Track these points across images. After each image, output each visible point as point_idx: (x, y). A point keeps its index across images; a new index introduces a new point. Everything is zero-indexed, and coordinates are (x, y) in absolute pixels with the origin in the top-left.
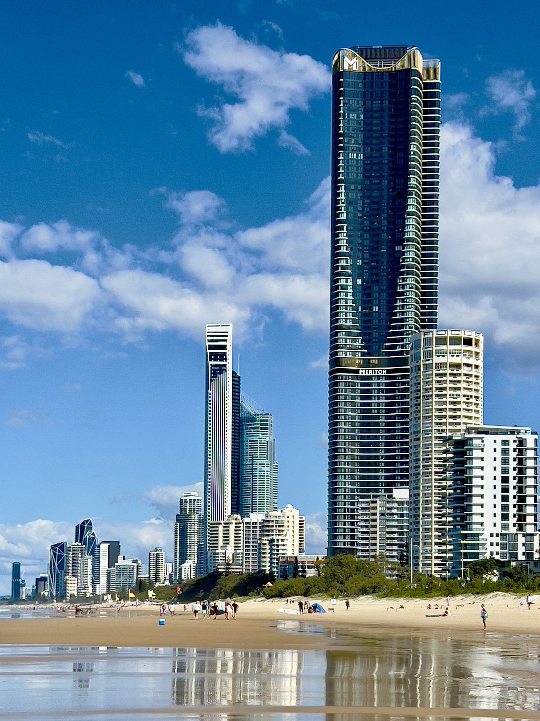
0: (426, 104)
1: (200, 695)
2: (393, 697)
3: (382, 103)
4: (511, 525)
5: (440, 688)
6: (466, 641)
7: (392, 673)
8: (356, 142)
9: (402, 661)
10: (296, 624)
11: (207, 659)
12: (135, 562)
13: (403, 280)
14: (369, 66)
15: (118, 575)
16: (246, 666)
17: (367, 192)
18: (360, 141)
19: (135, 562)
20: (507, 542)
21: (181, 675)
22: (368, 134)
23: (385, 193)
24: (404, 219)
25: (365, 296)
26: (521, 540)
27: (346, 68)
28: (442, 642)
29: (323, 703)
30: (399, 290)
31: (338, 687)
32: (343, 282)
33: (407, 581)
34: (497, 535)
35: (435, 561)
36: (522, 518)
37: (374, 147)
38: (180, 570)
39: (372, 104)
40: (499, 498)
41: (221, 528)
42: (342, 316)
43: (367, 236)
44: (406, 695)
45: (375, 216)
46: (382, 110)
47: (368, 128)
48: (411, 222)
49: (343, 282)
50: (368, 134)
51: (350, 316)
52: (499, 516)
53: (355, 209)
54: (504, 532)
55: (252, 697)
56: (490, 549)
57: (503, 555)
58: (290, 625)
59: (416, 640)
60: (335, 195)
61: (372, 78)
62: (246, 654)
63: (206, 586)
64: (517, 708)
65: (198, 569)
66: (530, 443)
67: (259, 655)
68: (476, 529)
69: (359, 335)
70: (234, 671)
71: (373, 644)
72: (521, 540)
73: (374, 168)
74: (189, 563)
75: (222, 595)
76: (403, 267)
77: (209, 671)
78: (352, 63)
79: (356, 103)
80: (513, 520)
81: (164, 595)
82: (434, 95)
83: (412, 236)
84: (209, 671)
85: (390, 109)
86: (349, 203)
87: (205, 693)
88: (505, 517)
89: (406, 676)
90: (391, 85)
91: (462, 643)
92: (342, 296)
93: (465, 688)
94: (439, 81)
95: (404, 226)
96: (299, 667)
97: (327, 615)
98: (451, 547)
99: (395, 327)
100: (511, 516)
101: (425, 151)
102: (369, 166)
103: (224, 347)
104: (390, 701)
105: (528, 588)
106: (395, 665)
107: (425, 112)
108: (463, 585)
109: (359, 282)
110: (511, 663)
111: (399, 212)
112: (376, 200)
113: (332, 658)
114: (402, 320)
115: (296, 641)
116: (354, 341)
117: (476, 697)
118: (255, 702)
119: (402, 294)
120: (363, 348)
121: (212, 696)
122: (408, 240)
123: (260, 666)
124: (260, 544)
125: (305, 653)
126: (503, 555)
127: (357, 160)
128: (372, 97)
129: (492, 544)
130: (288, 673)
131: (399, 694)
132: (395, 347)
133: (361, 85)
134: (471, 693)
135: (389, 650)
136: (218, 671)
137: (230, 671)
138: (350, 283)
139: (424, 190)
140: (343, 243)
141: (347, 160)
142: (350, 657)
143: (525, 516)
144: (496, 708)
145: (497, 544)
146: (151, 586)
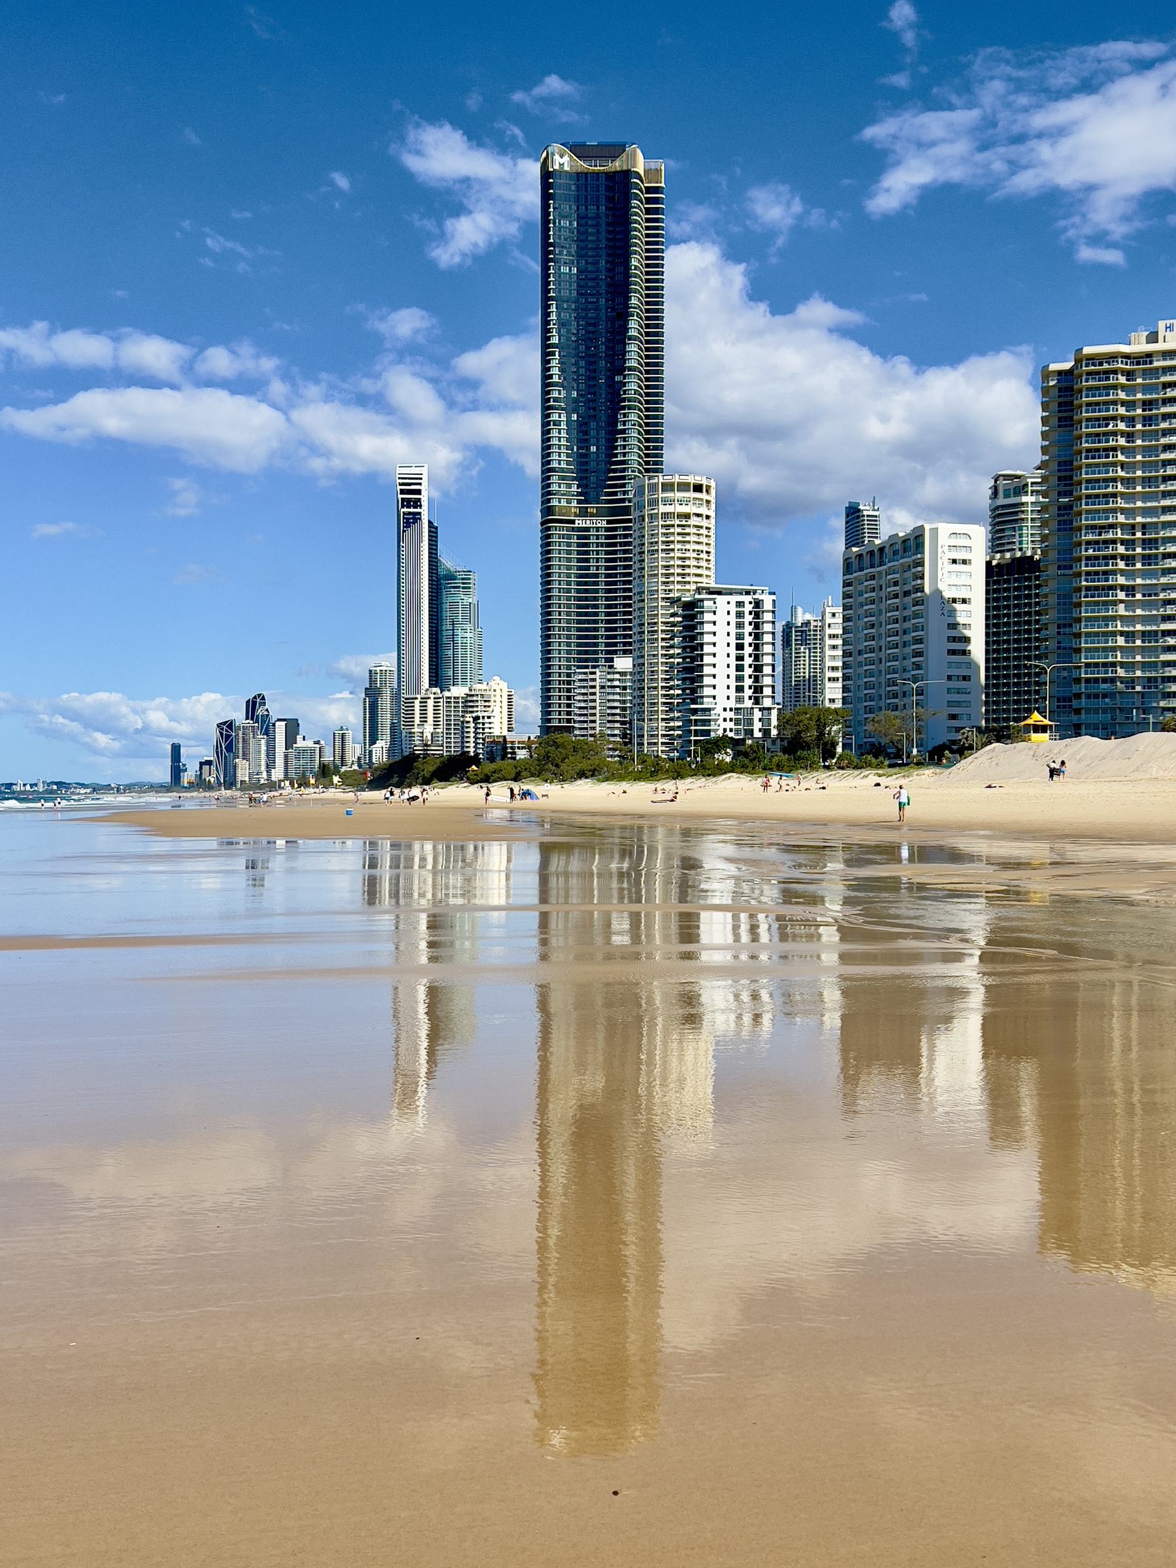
0: (648, 211)
1: (395, 894)
2: (615, 893)
3: (598, 209)
4: (746, 698)
5: (667, 882)
6: (696, 829)
7: (614, 866)
8: (569, 254)
9: (625, 853)
10: (506, 813)
11: (403, 854)
12: (317, 742)
13: (625, 415)
14: (583, 165)
15: (298, 758)
16: (448, 860)
17: (582, 313)
18: (573, 252)
19: (317, 742)
20: (742, 717)
21: (373, 871)
22: (583, 244)
23: (603, 314)
24: (625, 344)
25: (581, 433)
26: (757, 715)
27: (557, 167)
28: (670, 832)
29: (536, 901)
30: (620, 427)
31: (553, 882)
32: (555, 417)
33: (633, 763)
34: (731, 710)
35: (661, 740)
36: (758, 689)
37: (590, 260)
38: (370, 752)
39: (586, 209)
40: (733, 667)
41: (417, 703)
42: (555, 457)
43: (582, 363)
44: (629, 890)
45: (591, 340)
46: (598, 216)
47: (583, 237)
48: (632, 347)
49: (555, 417)
50: (583, 244)
51: (563, 457)
52: (733, 688)
53: (569, 331)
54: (739, 706)
55: (455, 896)
56: (724, 725)
57: (737, 732)
58: (497, 813)
59: (640, 828)
60: (546, 315)
61: (586, 180)
62: (448, 847)
63: (402, 770)
64: (753, 902)
65: (391, 751)
66: (768, 605)
67: (462, 848)
68: (707, 703)
69: (574, 479)
70: (434, 867)
71: (592, 834)
72: (757, 715)
73: (590, 284)
74: (379, 744)
75: (420, 780)
76: (624, 400)
77: (405, 867)
78: (563, 161)
79: (569, 208)
80: (748, 692)
81: (355, 781)
82: (656, 201)
83: (634, 364)
84: (405, 867)
85: (607, 216)
86: (562, 324)
87: (401, 892)
88: (740, 689)
89: (629, 869)
90: (608, 188)
91: (691, 830)
92: (554, 433)
93: (694, 880)
94: (663, 185)
95: (624, 353)
96: (509, 860)
97: (541, 803)
98: (680, 724)
99: (615, 471)
100: (746, 688)
101: (647, 266)
102: (584, 282)
103: (418, 492)
104: (611, 897)
105: (764, 769)
106: (617, 856)
107: (648, 220)
108: (693, 766)
109: (574, 417)
110: (747, 852)
111: (619, 336)
112: (592, 321)
113: (546, 850)
114: (623, 462)
115: (507, 831)
116: (569, 486)
117: (707, 891)
118: (460, 901)
119: (623, 431)
120: (579, 494)
121: (409, 895)
122: (630, 369)
123: (463, 861)
124: (463, 722)
125: (516, 846)
126: (737, 732)
127: (570, 275)
128: (586, 201)
129: (725, 720)
130: (496, 868)
131: (621, 890)
132: (615, 494)
133: (573, 187)
134: (703, 886)
135: (611, 840)
136: (416, 867)
137: (429, 867)
138: (563, 418)
139: (647, 311)
140: (555, 371)
141: (559, 274)
142: (567, 848)
143: (762, 687)
144: (730, 902)
145: (731, 720)
146: (336, 771)
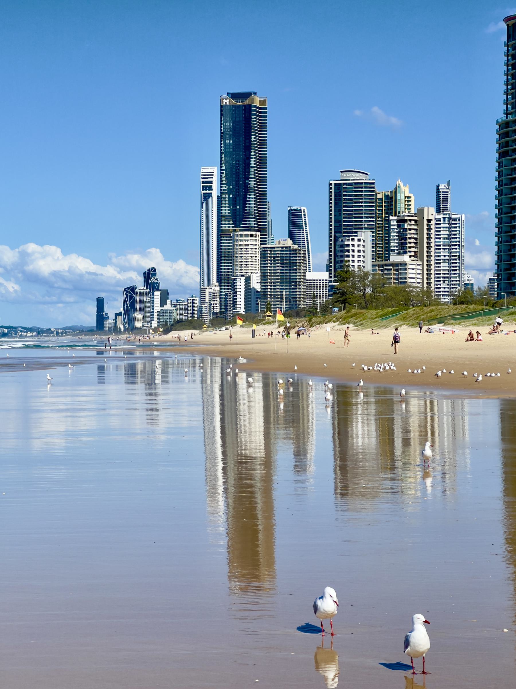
13: (249, 195)
25: (233, 202)
27: (224, 104)
30: (248, 199)
32: (223, 196)
42: (223, 211)
43: (234, 176)
48: (252, 170)
51: (227, 211)
69: (230, 218)
76: (249, 190)
83: (253, 176)
95: (249, 172)
99: (246, 216)
109: (231, 196)
114: (249, 212)
116: (229, 221)
119: (249, 201)
120: (232, 224)
122: (251, 178)
132: (246, 224)
138: (227, 196)
140: (224, 179)
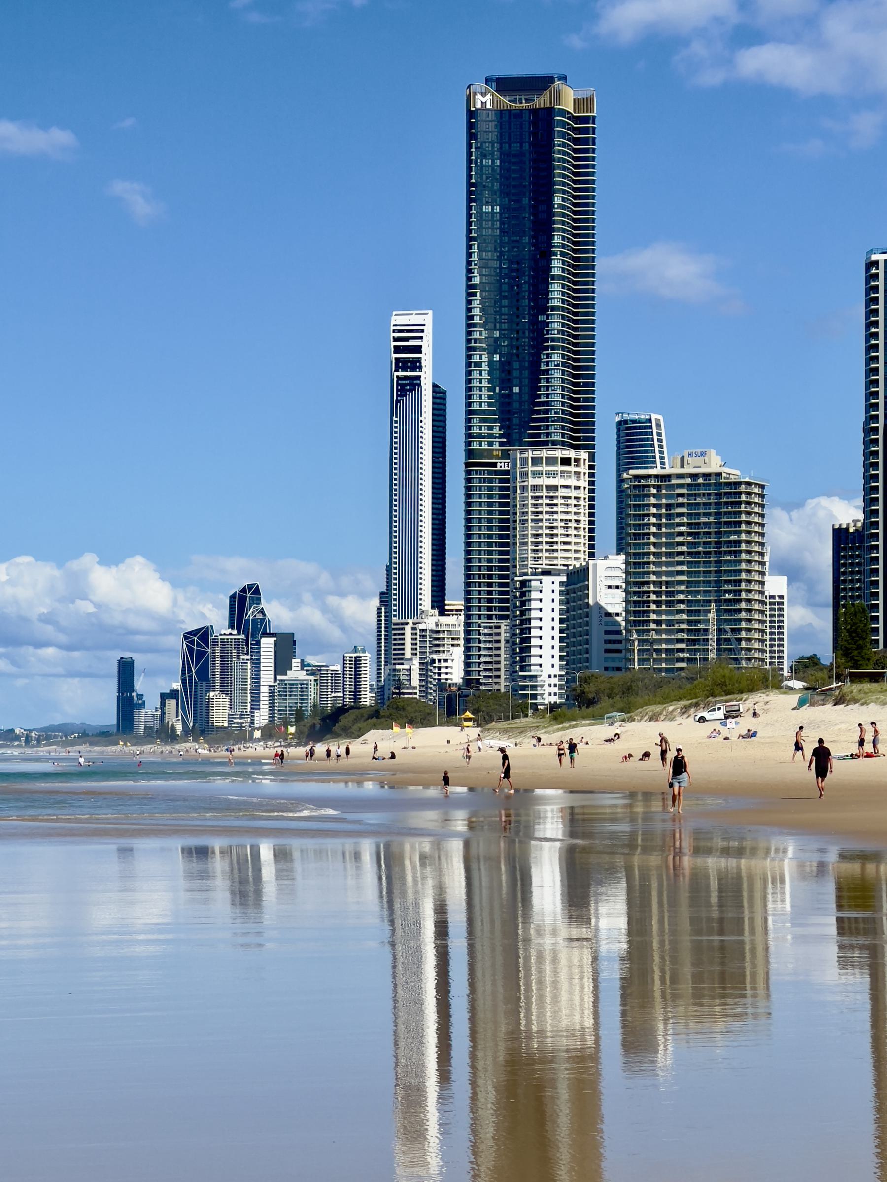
3: (521, 146)
13: (548, 356)
24: (548, 284)
25: (503, 375)
30: (543, 367)
32: (476, 358)
37: (513, 198)
39: (510, 146)
42: (476, 399)
48: (556, 287)
49: (476, 358)
51: (485, 399)
69: (495, 421)
76: (547, 340)
83: (556, 303)
90: (534, 123)
92: (475, 375)
95: (547, 292)
99: (538, 412)
109: (497, 357)
114: (547, 403)
116: (490, 428)
119: (547, 372)
120: (501, 436)
122: (553, 308)
132: (539, 435)
138: (485, 358)
140: (477, 312)
141: (480, 213)
